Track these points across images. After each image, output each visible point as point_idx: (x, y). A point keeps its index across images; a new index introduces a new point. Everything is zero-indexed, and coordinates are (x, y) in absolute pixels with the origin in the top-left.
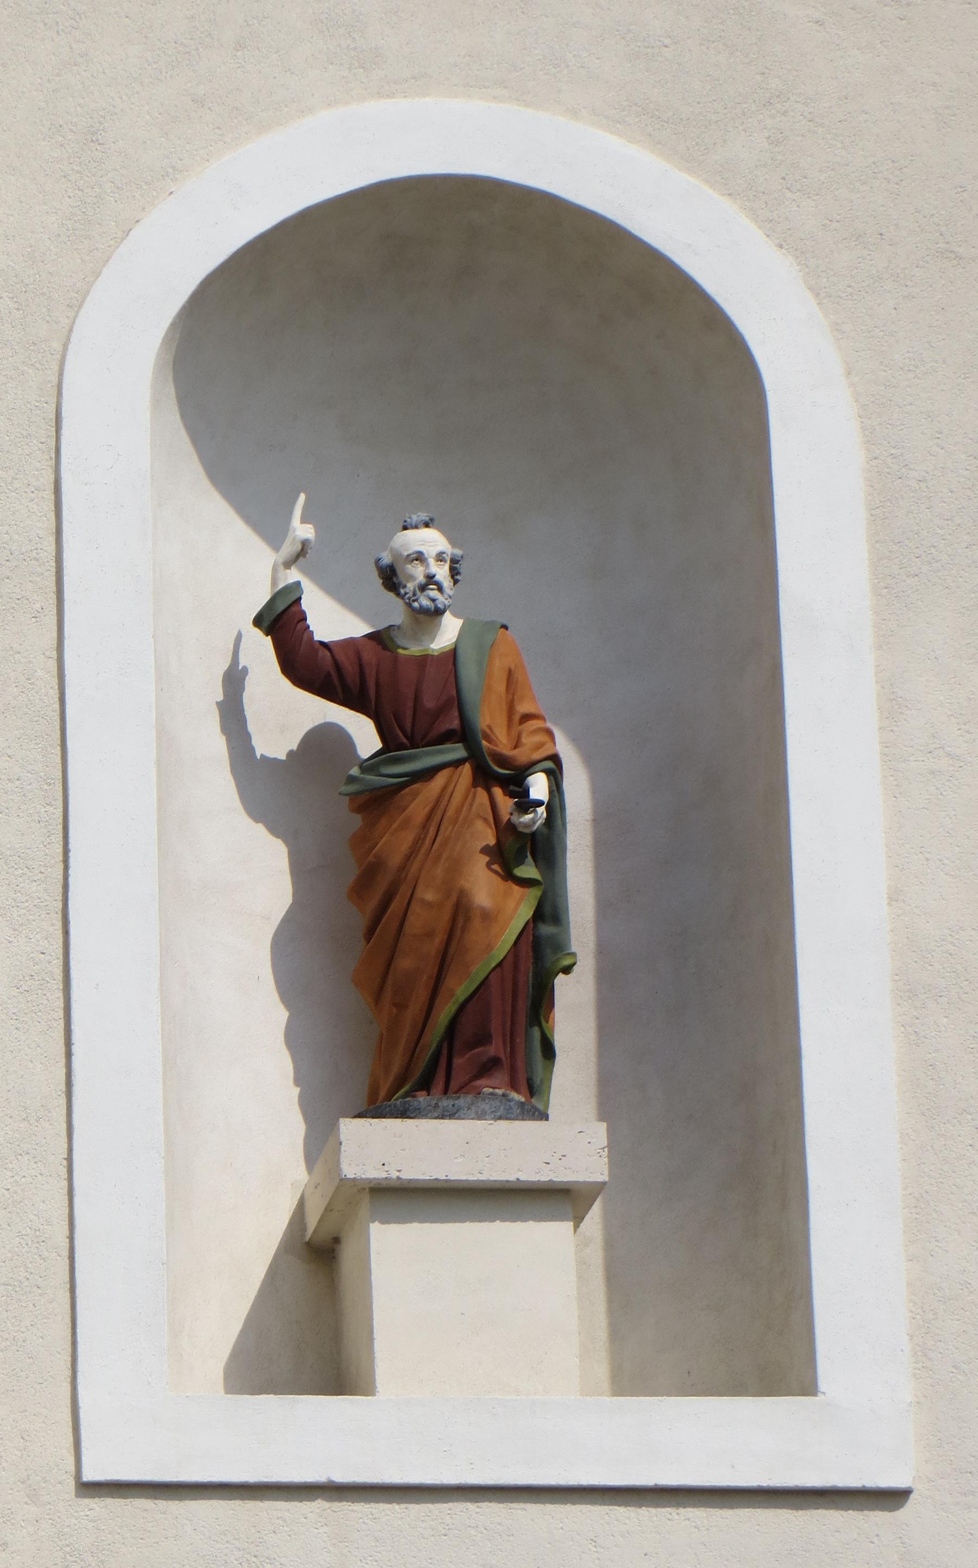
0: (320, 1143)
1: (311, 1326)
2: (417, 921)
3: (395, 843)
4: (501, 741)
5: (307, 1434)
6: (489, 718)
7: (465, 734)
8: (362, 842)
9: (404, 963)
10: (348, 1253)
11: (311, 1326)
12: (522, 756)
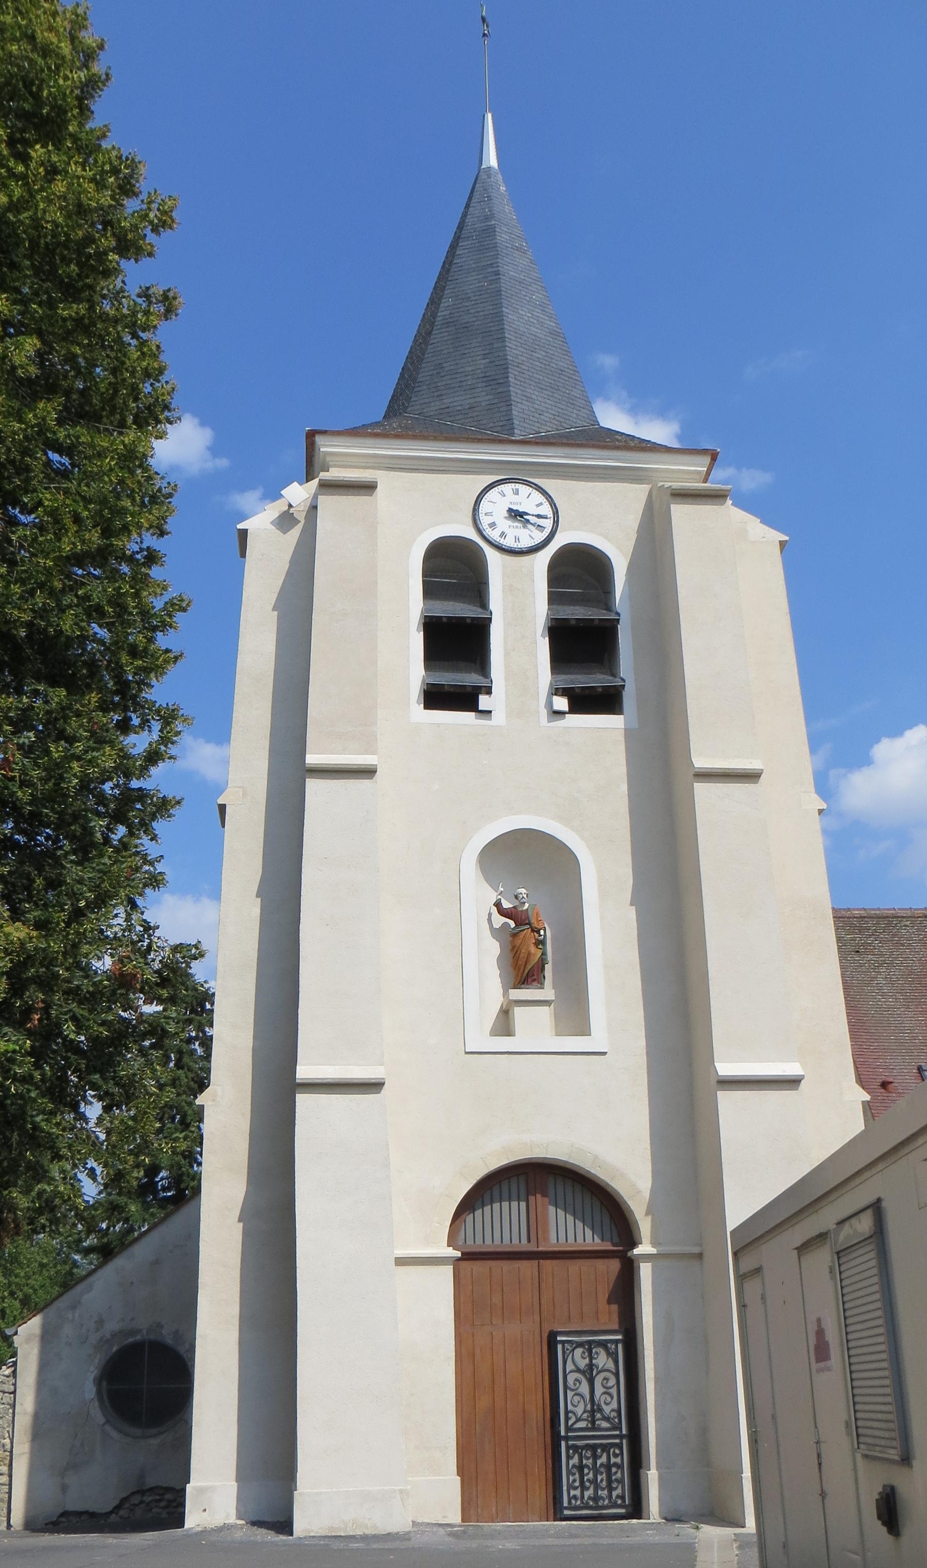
0: (506, 993)
1: (504, 1025)
2: (521, 956)
3: (518, 942)
4: (535, 925)
5: (504, 1044)
6: (533, 921)
7: (529, 924)
8: (512, 942)
9: (520, 963)
10: (511, 1012)
11: (504, 1025)
12: (539, 927)
